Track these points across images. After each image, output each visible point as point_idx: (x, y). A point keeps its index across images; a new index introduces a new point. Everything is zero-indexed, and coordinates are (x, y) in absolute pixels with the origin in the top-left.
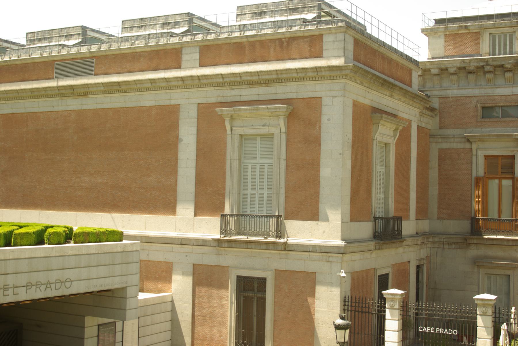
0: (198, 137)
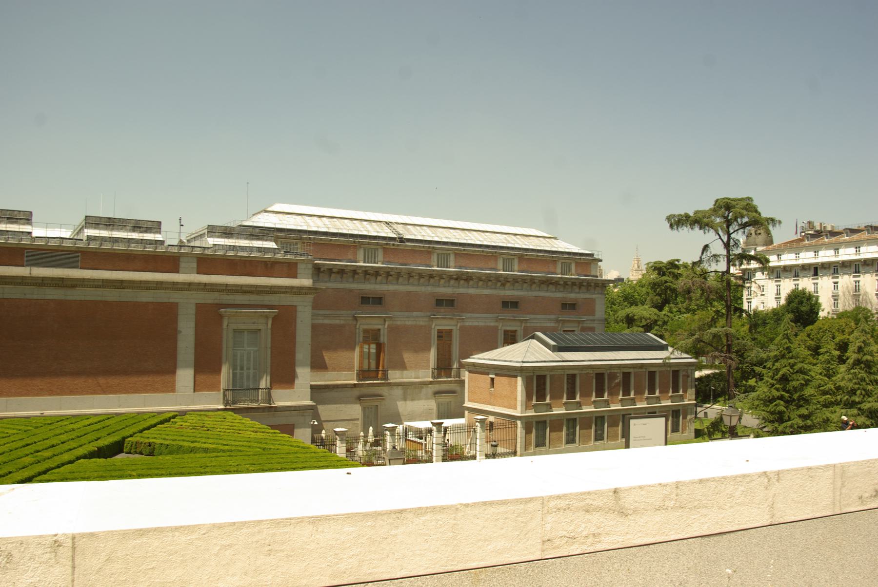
0: (196, 330)
